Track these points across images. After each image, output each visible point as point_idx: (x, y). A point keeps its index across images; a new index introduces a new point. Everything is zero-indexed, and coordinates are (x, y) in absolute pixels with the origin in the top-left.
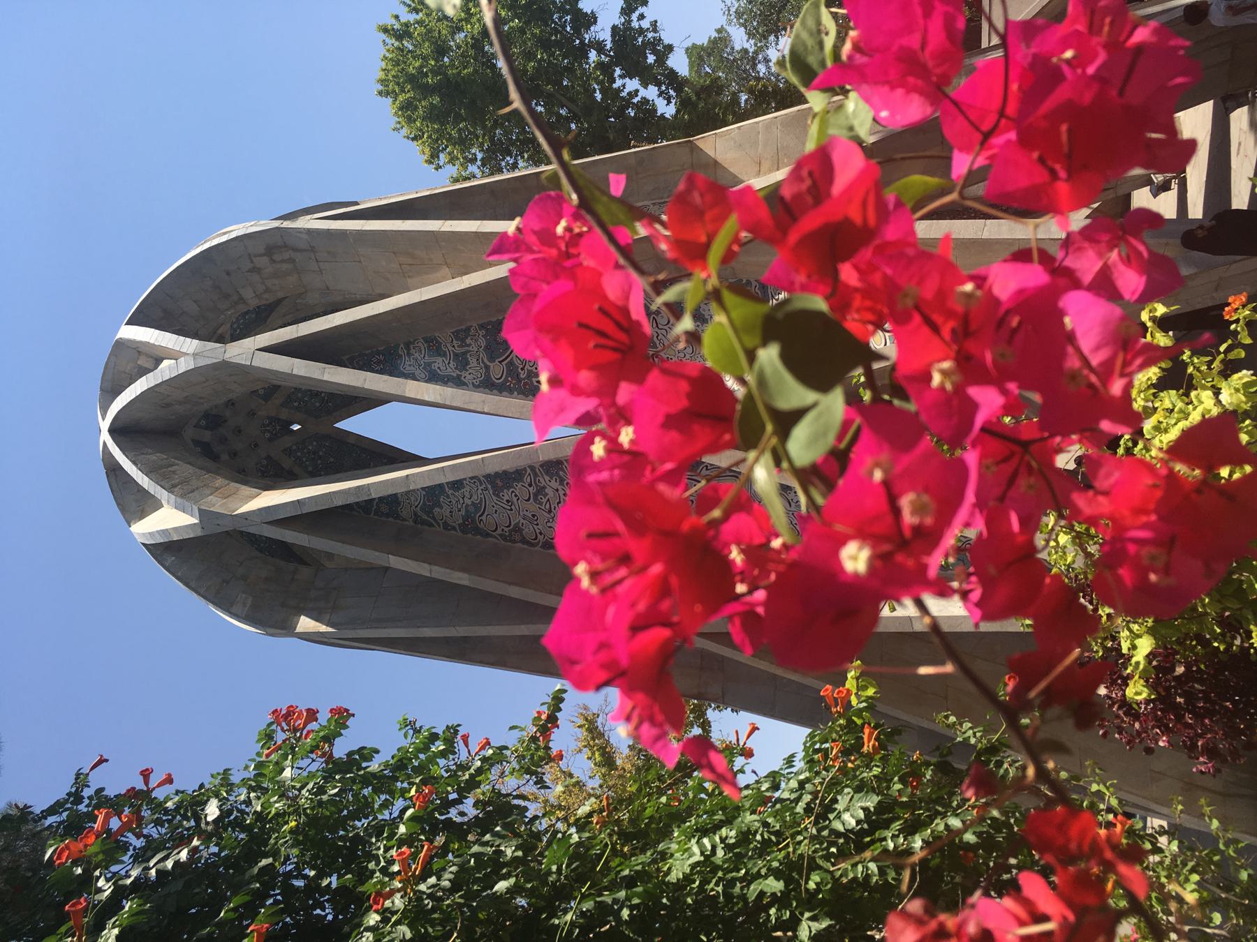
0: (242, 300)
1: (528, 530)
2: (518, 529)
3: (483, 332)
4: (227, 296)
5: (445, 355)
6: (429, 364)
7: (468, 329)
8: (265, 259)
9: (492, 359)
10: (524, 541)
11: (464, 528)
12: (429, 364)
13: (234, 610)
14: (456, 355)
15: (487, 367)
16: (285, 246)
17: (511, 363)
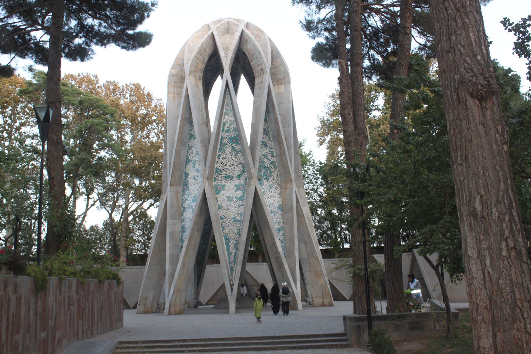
0: (252, 61)
1: (190, 151)
2: (191, 149)
6: (227, 122)
7: (236, 131)
9: (228, 139)
10: (188, 150)
11: (190, 134)
13: (172, 70)
16: (263, 74)
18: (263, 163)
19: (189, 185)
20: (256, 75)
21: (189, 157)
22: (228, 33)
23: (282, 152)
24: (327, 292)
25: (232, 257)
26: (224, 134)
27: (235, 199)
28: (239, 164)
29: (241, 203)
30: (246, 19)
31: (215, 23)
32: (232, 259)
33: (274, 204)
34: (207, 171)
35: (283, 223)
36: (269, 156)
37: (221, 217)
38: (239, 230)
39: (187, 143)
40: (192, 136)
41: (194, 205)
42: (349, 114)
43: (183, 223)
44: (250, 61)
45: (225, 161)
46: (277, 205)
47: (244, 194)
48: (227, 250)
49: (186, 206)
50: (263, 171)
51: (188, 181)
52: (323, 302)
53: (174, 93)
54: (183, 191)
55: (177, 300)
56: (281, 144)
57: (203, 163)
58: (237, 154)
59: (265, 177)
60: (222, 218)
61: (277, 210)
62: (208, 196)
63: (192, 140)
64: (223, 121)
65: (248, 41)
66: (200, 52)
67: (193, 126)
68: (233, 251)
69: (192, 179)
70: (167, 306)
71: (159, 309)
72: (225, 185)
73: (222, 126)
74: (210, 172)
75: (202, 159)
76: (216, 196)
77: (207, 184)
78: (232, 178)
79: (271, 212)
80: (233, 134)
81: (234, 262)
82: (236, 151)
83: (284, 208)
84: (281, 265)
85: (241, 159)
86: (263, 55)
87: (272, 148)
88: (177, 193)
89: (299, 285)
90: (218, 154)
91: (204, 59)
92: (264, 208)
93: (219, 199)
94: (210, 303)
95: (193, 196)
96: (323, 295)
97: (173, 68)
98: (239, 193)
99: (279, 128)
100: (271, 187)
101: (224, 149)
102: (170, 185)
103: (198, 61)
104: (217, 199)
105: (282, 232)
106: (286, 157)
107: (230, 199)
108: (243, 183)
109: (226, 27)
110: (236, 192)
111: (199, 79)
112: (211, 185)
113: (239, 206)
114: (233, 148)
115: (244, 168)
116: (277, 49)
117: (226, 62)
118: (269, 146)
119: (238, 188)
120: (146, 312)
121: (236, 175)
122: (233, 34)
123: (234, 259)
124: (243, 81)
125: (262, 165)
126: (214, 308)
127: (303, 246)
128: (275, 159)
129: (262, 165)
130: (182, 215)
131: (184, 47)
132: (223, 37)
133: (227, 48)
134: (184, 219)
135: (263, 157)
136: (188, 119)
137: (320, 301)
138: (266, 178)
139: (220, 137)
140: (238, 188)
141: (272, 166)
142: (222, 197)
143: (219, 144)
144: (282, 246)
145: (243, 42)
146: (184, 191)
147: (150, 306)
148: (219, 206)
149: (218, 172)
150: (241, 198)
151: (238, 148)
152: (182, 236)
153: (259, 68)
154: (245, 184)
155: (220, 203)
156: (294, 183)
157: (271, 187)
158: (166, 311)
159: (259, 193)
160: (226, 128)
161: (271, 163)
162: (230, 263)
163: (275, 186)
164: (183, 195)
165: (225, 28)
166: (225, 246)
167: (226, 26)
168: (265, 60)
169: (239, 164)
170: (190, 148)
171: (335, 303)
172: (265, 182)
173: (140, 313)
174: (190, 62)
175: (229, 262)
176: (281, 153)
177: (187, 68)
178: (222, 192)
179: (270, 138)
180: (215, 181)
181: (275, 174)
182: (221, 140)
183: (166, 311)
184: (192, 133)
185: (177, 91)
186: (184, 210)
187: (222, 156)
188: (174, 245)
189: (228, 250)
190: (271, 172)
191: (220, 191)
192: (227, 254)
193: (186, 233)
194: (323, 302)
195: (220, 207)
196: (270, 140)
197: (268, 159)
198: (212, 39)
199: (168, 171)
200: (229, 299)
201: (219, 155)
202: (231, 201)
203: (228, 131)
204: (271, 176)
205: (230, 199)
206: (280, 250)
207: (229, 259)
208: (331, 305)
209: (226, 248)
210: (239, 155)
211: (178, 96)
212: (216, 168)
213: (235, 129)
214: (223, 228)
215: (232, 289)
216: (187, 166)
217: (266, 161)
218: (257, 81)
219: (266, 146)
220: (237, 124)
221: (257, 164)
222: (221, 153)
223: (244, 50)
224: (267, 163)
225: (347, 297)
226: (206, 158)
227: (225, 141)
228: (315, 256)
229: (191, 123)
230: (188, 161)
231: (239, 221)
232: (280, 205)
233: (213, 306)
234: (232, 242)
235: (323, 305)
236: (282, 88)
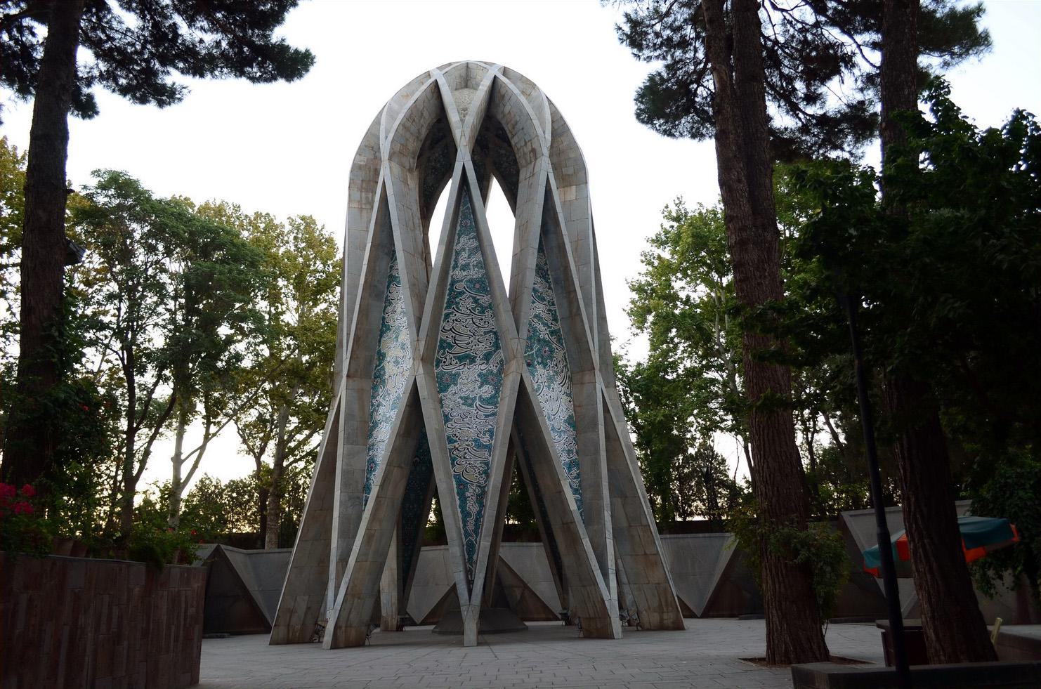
0: (513, 136)
1: (389, 309)
3: (480, 276)
4: (514, 128)
5: (469, 258)
6: (464, 250)
7: (482, 268)
8: (530, 148)
10: (386, 307)
11: (391, 276)
12: (464, 250)
14: (468, 264)
15: (462, 281)
16: (536, 159)
17: (464, 293)
18: (535, 330)
19: (386, 377)
20: (522, 162)
21: (387, 320)
22: (466, 86)
23: (574, 310)
24: (670, 599)
25: (471, 521)
26: (458, 274)
27: (478, 403)
28: (486, 333)
29: (490, 409)
30: (502, 62)
31: (440, 68)
32: (471, 527)
33: (559, 414)
34: (422, 344)
35: (577, 453)
36: (547, 317)
37: (448, 437)
39: (383, 292)
40: (392, 279)
41: (393, 414)
42: (739, 181)
43: (371, 453)
44: (510, 136)
45: (457, 326)
46: (563, 416)
47: (497, 391)
48: (460, 506)
49: (379, 418)
50: (536, 347)
51: (383, 368)
52: (662, 620)
53: (360, 202)
54: (373, 389)
55: (351, 616)
56: (572, 295)
57: (414, 329)
58: (483, 312)
59: (540, 360)
60: (450, 441)
61: (563, 426)
62: (423, 393)
63: (393, 287)
64: (457, 247)
65: (507, 98)
66: (410, 116)
67: (396, 259)
68: (473, 507)
69: (392, 364)
70: (330, 627)
71: (308, 634)
72: (457, 375)
73: (454, 257)
74: (427, 348)
75: (412, 319)
76: (440, 396)
77: (421, 370)
78: (473, 360)
79: (553, 429)
80: (475, 273)
82: (481, 307)
83: (579, 423)
84: (575, 540)
85: (491, 322)
86: (536, 122)
87: (553, 304)
88: (361, 391)
89: (613, 584)
90: (444, 313)
91: (419, 133)
92: (540, 419)
93: (446, 402)
94: (431, 620)
95: (392, 398)
96: (660, 605)
97: (359, 153)
98: (487, 390)
99: (569, 263)
100: (551, 380)
101: (457, 304)
102: (348, 376)
103: (408, 135)
104: (441, 401)
105: (575, 471)
106: (582, 321)
107: (469, 402)
108: (495, 371)
109: (464, 75)
110: (480, 387)
111: (410, 170)
112: (428, 373)
113: (486, 416)
114: (476, 301)
115: (497, 339)
116: (562, 118)
117: (463, 131)
118: (548, 298)
119: (484, 378)
120: (289, 641)
121: (480, 355)
122: (475, 88)
124: (496, 188)
125: (533, 336)
126: (433, 631)
127: (618, 501)
128: (559, 326)
129: (533, 336)
130: (370, 436)
131: (381, 113)
132: (456, 93)
133: (465, 110)
134: (373, 445)
135: (536, 320)
136: (384, 246)
137: (655, 618)
138: (542, 363)
139: (450, 278)
140: (484, 378)
141: (554, 339)
142: (453, 397)
143: (448, 291)
144: (577, 500)
145: (497, 101)
146: (375, 388)
147: (298, 627)
148: (446, 416)
149: (444, 349)
150: (492, 401)
151: (484, 300)
152: (368, 479)
153: (527, 149)
154: (500, 371)
155: (447, 410)
156: (597, 373)
157: (551, 380)
158: (328, 638)
159: (529, 390)
160: (461, 262)
161: (552, 333)
162: (467, 534)
163: (559, 380)
164: (374, 397)
165: (461, 76)
166: (457, 497)
167: (463, 72)
168: (540, 131)
169: (486, 333)
170: (388, 302)
171: (687, 623)
172: (540, 370)
173: (278, 644)
174: (391, 136)
175: (466, 531)
176: (571, 312)
177: (385, 147)
178: (452, 389)
179: (549, 283)
180: (437, 366)
181: (559, 355)
182: (452, 285)
183: (328, 638)
184: (394, 273)
185: (367, 198)
186: (375, 425)
187: (452, 317)
188: (350, 498)
189: (463, 506)
190: (552, 351)
191: (449, 386)
192: (460, 515)
193: (376, 473)
194: (662, 620)
195: (447, 419)
196: (550, 288)
197: (545, 325)
198: (435, 95)
199: (345, 348)
200: (464, 613)
201: (447, 316)
202: (471, 405)
203: (465, 267)
204: (551, 358)
205: (469, 402)
206: (573, 506)
207: (465, 526)
208: (679, 627)
209: (458, 502)
210: (488, 314)
211: (368, 206)
212: (441, 340)
213: (479, 263)
214: (453, 460)
215: (470, 592)
216: (383, 339)
217: (542, 328)
218: (523, 174)
219: (543, 299)
220: (483, 254)
221: (524, 333)
222: (451, 310)
223: (499, 117)
224: (544, 333)
225: (698, 612)
226: (419, 320)
227: (460, 287)
228: (644, 522)
229: (392, 254)
230: (384, 328)
231: (487, 446)
232: (570, 417)
233: (432, 627)
234: (471, 491)
235: (661, 627)
236: (572, 193)
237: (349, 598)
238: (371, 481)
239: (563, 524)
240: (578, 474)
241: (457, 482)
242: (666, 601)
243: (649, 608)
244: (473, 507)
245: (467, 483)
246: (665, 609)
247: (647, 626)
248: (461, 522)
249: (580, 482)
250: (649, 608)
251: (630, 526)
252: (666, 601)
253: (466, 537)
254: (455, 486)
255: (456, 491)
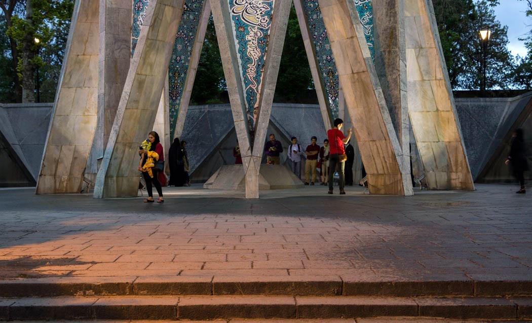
32: (251, 74)
38: (270, 5)
48: (240, 51)
55: (122, 166)
68: (254, 52)
81: (257, 79)
105: (367, 16)
123: (257, 72)
147: (66, 177)
152: (135, 21)
166: (236, 41)
175: (246, 78)
192: (240, 61)
194: (449, 180)
207: (245, 72)
209: (237, 47)
237: (120, 147)
238: (138, 23)
239: (353, 73)
240: (371, 20)
241: (236, 24)
242: (456, 161)
243: (437, 167)
244: (254, 52)
245: (248, 26)
246: (454, 169)
247: (433, 185)
248: (241, 68)
249: (373, 28)
250: (437, 167)
251: (423, 80)
252: (456, 161)
253: (246, 85)
254: (234, 28)
255: (234, 33)
